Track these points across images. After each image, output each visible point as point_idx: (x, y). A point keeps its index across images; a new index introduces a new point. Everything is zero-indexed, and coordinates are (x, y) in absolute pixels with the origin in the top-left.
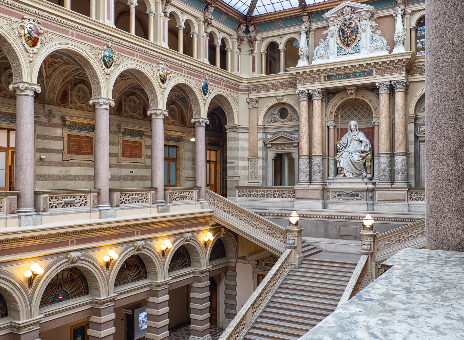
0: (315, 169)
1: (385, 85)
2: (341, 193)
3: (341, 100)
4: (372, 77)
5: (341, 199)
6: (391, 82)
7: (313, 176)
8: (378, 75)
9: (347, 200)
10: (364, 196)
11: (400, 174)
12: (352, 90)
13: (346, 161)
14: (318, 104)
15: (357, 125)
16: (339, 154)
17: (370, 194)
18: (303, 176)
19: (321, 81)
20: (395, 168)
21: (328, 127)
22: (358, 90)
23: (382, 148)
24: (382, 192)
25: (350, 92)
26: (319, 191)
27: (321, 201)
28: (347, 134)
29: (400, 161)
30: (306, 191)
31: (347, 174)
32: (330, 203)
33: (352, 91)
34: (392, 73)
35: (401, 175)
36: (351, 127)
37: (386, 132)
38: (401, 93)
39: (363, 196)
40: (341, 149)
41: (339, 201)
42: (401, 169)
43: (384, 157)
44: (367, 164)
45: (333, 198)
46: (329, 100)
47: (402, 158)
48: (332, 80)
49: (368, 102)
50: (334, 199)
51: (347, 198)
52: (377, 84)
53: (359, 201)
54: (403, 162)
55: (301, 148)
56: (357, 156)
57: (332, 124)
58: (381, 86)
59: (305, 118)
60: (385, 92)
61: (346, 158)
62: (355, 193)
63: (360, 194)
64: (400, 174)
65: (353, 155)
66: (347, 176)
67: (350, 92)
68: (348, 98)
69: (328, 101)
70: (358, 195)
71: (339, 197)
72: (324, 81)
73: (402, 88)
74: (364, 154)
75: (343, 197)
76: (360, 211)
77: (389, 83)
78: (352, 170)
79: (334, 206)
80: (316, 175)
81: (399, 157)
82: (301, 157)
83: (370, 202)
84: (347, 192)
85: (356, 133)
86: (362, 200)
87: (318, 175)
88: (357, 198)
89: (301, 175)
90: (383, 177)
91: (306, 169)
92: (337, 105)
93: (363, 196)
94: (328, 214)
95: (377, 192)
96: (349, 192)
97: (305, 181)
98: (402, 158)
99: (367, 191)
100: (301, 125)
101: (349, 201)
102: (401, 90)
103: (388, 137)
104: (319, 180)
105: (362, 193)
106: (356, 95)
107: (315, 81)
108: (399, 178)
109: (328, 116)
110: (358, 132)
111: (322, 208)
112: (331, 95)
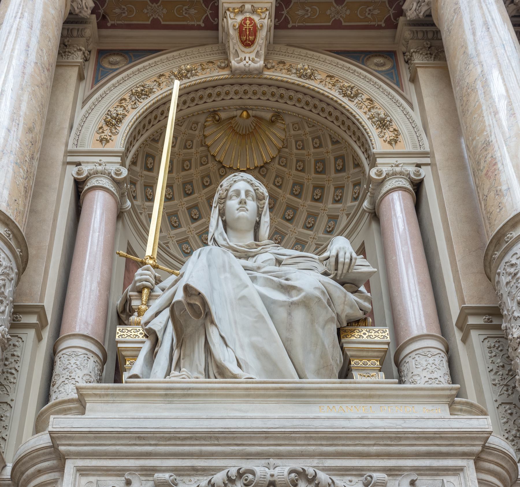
22: (277, 47)
69: (96, 80)
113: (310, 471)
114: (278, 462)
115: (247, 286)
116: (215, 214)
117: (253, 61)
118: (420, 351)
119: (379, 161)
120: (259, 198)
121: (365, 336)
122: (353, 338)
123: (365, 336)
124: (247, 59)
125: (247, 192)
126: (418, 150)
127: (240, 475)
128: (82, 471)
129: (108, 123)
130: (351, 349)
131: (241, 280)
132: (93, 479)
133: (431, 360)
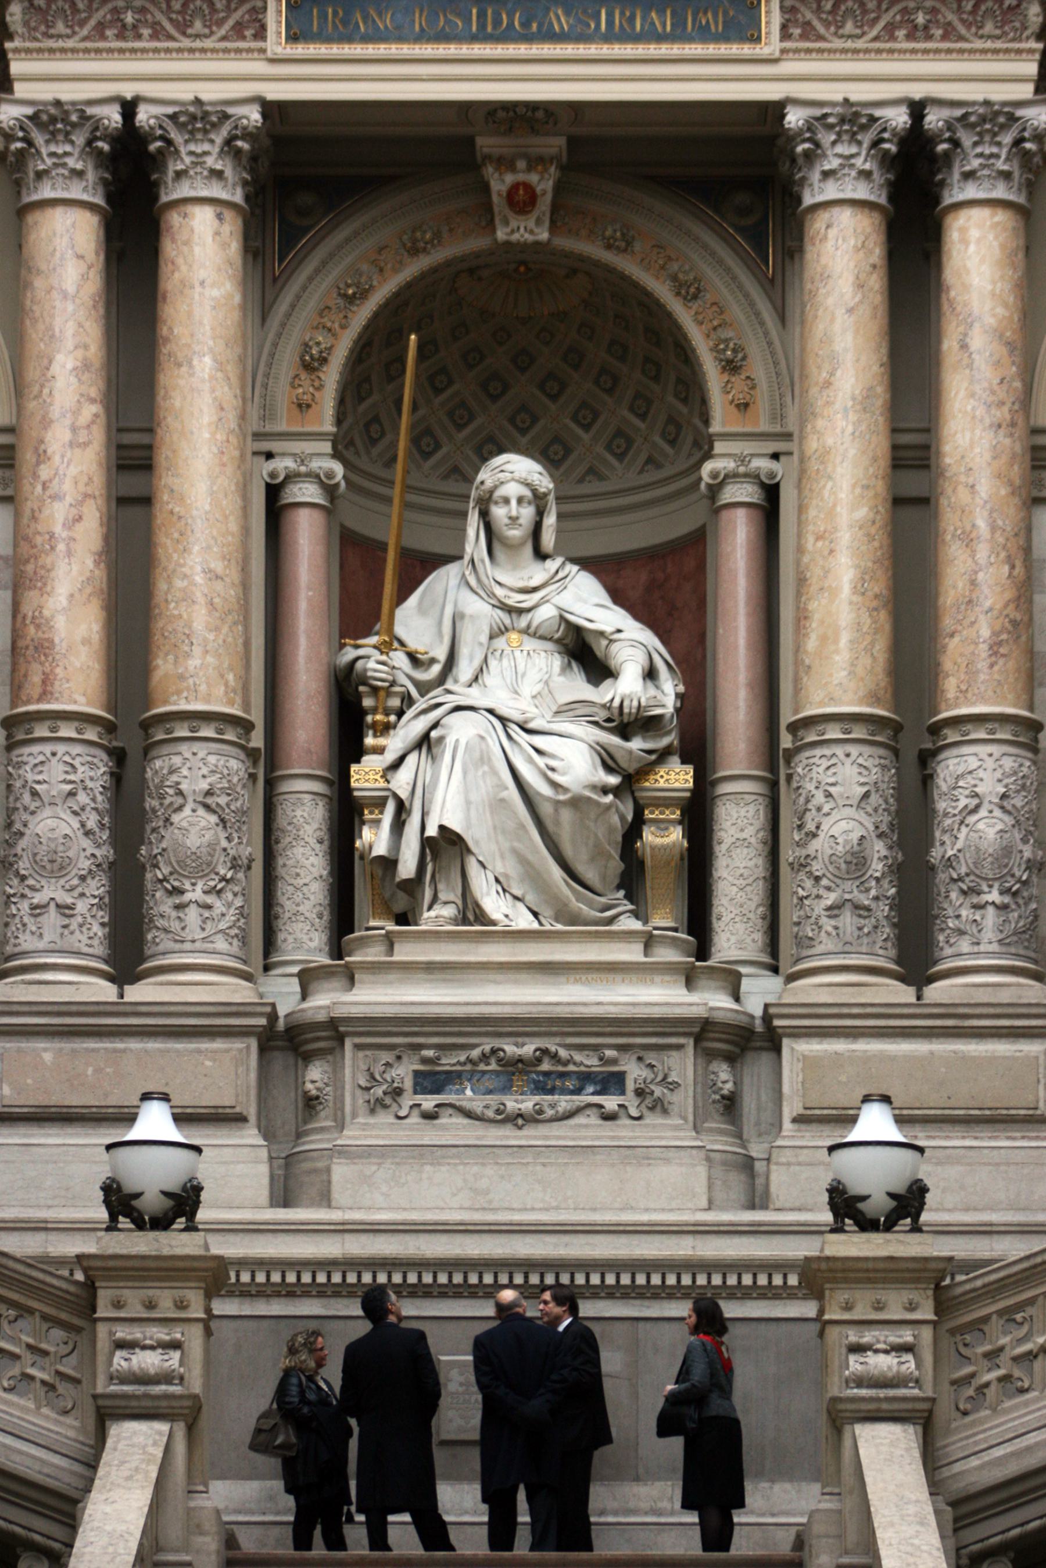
0: (194, 841)
1: (867, 138)
2: (449, 1062)
3: (414, 251)
4: (746, 50)
5: (449, 1120)
6: (917, 109)
7: (162, 905)
8: (804, 37)
9: (518, 1120)
10: (674, 1087)
11: (994, 896)
12: (536, 162)
13: (483, 790)
14: (224, 246)
15: (551, 497)
16: (412, 728)
17: (723, 1073)
18: (65, 910)
19: (261, 33)
20: (936, 854)
21: (273, 492)
23: (840, 675)
24: (839, 1046)
25: (510, 179)
26: (237, 1045)
27: (250, 1135)
28: (445, 579)
29: (990, 786)
30: (91, 1044)
31: (494, 905)
32: (342, 1152)
33: (533, 178)
34: (929, 38)
35: (1003, 908)
36: (499, 512)
37: (871, 538)
38: (1001, 216)
39: (658, 1091)
40: (395, 702)
41: (429, 1135)
42: (1007, 851)
43: (854, 750)
44: (650, 836)
45: (376, 1106)
46: (289, 239)
47: (1008, 763)
48: (366, 39)
49: (662, 291)
50: (385, 1118)
51: (512, 1104)
52: (794, 118)
53: (624, 1132)
54: (1018, 802)
55: (44, 648)
56: (585, 747)
57: (315, 465)
58: (827, 138)
59: (86, 366)
60: (862, 191)
61: (484, 759)
62: (590, 1062)
63: (634, 1072)
64: (994, 896)
65: (539, 741)
66: (495, 915)
67: (510, 179)
68: (476, 243)
70: (612, 1082)
71: (429, 1102)
72: (293, 38)
73: (1007, 176)
74: (636, 744)
75: (469, 1096)
76: (645, 1218)
77: (899, 118)
78: (533, 875)
79: (382, 1172)
80: (195, 893)
81: (983, 750)
82: (41, 731)
83: (720, 1144)
84: (510, 1049)
85: (538, 573)
86: (651, 1119)
87: (219, 906)
88: (611, 1103)
89: (38, 898)
90: (848, 920)
91: (86, 843)
92: (363, 294)
93: (658, 1091)
94: (329, 1248)
95: (794, 1050)
96: (528, 1049)
97: (78, 953)
98: (1008, 763)
99: (698, 1039)
100: (46, 423)
101: (532, 1135)
102: (1000, 192)
103: (879, 586)
104: (221, 944)
105: (651, 1058)
106: (553, 228)
107: (198, 25)
108: (989, 933)
109: (283, 394)
110: (552, 565)
111: (263, 1194)
112: (306, 199)
113: (553, 1049)
114: (526, 1040)
115: (506, 788)
116: (473, 519)
117: (532, 232)
118: (732, 797)
119: (719, 447)
120: (539, 500)
121: (662, 781)
122: (647, 784)
123: (662, 781)
124: (522, 230)
125: (520, 500)
126: (778, 429)
127: (494, 1051)
128: (358, 1047)
129: (308, 367)
130: (643, 798)
131: (500, 778)
132: (368, 1053)
133: (743, 813)
